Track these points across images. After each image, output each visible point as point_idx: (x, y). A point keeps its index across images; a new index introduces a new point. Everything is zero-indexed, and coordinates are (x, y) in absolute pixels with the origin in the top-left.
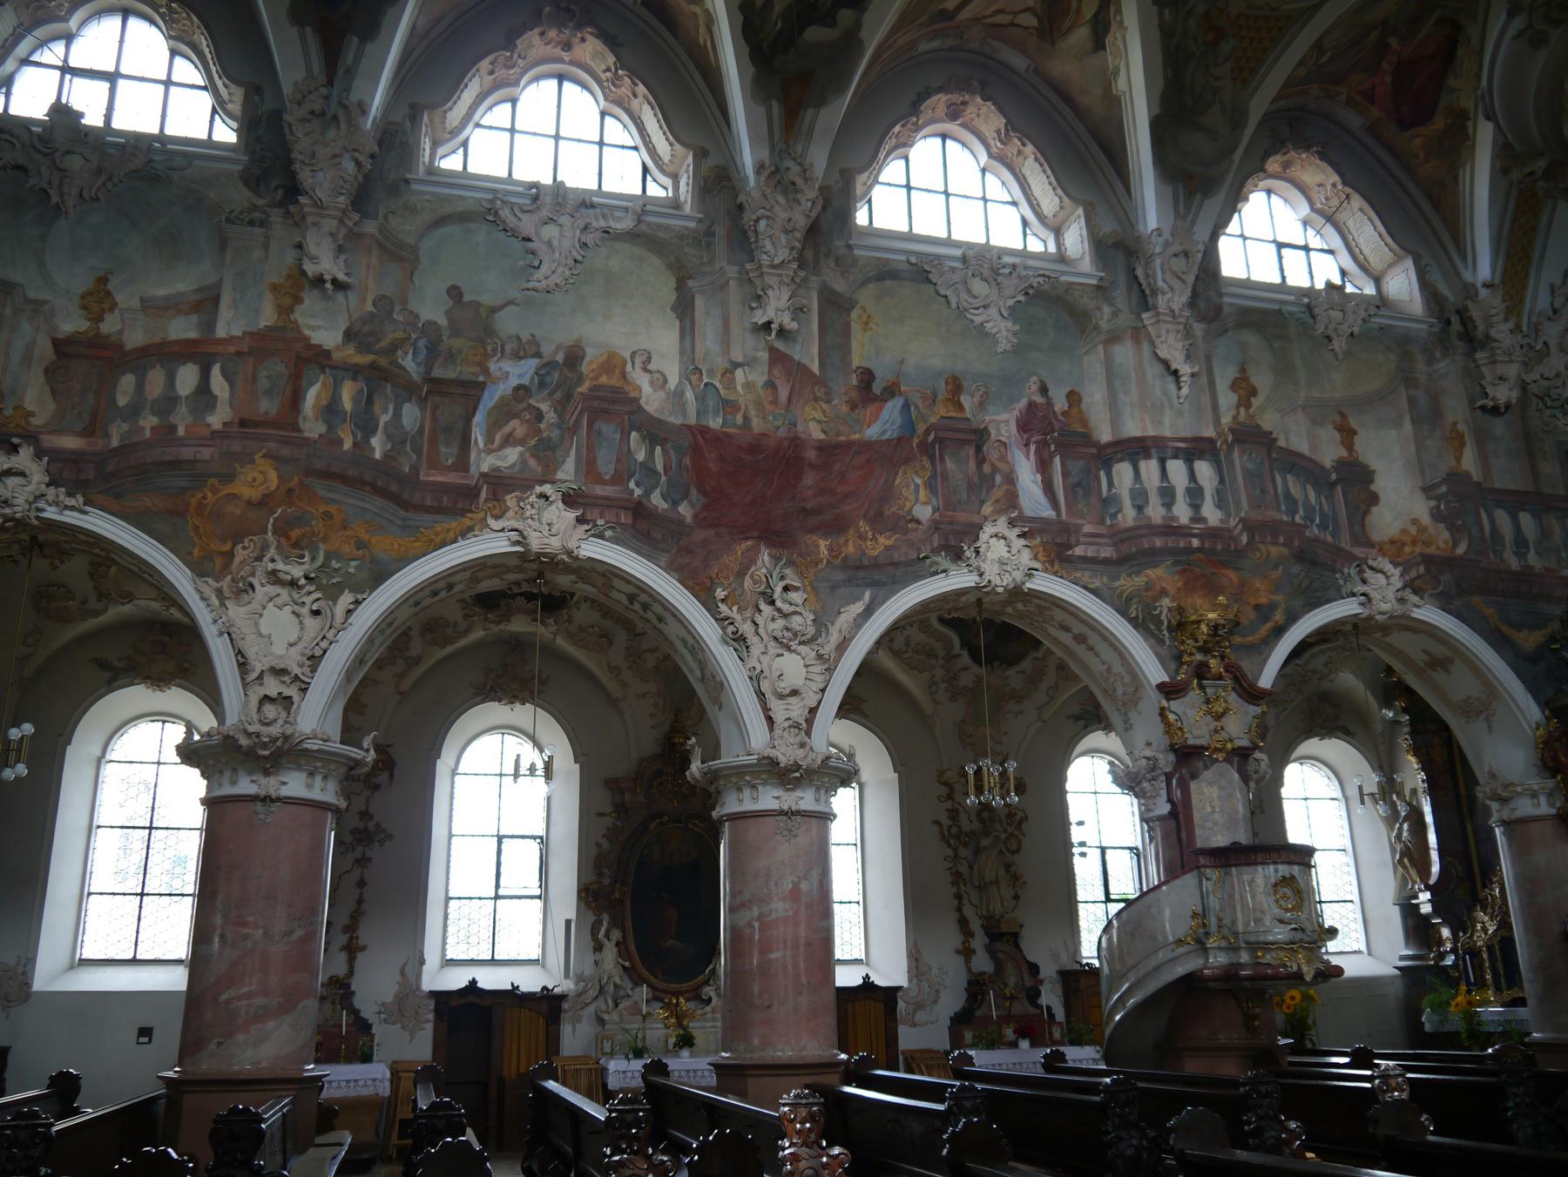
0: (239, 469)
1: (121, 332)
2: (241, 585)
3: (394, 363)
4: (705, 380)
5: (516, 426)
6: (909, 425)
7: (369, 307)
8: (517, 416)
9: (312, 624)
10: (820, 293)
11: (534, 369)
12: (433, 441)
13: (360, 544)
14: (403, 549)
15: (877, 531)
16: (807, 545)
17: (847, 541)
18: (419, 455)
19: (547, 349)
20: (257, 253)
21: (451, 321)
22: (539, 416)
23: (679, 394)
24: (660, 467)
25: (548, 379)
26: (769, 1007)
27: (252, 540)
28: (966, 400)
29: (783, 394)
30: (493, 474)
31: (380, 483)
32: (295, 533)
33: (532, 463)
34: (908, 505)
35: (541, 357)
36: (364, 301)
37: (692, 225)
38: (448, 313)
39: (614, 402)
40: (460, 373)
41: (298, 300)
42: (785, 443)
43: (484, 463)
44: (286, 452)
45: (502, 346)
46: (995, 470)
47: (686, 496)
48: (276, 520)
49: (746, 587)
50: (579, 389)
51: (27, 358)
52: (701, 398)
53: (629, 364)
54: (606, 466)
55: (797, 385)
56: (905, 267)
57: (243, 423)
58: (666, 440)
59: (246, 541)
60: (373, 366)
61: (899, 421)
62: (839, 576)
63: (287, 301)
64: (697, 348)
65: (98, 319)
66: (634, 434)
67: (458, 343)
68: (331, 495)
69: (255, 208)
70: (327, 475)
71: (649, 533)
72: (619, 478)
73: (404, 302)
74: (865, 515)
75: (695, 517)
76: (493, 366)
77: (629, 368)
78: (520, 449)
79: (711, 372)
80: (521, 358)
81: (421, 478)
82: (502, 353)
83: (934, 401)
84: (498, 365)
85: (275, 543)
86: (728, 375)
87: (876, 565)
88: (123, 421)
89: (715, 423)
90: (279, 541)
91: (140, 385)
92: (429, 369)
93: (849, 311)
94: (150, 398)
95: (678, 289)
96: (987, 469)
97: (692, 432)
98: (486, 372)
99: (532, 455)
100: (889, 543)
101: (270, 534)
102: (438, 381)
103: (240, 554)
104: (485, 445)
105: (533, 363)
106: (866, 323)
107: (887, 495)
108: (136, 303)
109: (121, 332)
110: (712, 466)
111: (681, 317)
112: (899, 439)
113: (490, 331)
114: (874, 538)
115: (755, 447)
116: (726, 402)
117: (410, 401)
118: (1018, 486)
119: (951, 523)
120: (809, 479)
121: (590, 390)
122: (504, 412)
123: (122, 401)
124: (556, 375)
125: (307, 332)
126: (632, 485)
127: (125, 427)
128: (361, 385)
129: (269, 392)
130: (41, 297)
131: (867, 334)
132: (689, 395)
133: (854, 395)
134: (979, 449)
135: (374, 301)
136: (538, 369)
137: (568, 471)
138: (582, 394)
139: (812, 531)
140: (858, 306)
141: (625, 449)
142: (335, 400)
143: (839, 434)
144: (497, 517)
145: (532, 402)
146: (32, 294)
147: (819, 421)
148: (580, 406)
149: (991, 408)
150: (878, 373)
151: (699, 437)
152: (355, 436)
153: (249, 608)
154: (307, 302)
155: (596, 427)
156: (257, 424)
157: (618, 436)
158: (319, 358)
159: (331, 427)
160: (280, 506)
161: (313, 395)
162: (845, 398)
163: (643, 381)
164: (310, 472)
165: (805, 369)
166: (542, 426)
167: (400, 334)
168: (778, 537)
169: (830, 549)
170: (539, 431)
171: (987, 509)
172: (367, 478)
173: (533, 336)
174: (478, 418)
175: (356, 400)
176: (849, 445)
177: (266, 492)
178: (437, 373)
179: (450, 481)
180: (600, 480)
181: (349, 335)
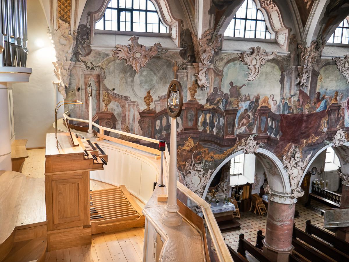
0: (185, 143)
1: (155, 108)
2: (187, 172)
3: (218, 107)
4: (285, 101)
5: (244, 121)
6: (326, 107)
7: (212, 91)
8: (244, 118)
9: (203, 179)
10: (312, 72)
11: (249, 104)
12: (227, 128)
13: (212, 157)
14: (221, 157)
15: (315, 136)
16: (302, 142)
17: (309, 139)
18: (224, 132)
19: (252, 98)
20: (185, 78)
21: (231, 93)
22: (249, 117)
23: (279, 106)
24: (274, 127)
25: (252, 107)
26: (283, 241)
27: (189, 160)
28: (338, 98)
29: (301, 103)
30: (240, 134)
31: (215, 141)
32: (198, 157)
33: (247, 130)
34: (323, 128)
35: (250, 100)
36: (211, 90)
37: (286, 55)
38: (230, 90)
39: (265, 110)
40: (233, 107)
41: (195, 92)
42: (300, 116)
43: (238, 132)
44: (195, 136)
45: (242, 98)
46: (341, 116)
47: (278, 133)
48: (194, 154)
49: (289, 154)
50: (258, 108)
51: (134, 119)
52: (284, 107)
53: (269, 99)
54: (263, 129)
55: (304, 100)
56: (331, 61)
57: (185, 130)
58: (275, 119)
59: (188, 161)
60: (213, 109)
61: (324, 106)
62: (307, 148)
63: (193, 92)
64: (284, 92)
65: (149, 105)
66: (269, 119)
67: (232, 99)
68: (205, 146)
69: (184, 64)
70: (204, 141)
71: (270, 144)
72: (265, 131)
73: (220, 88)
74: (314, 132)
75: (280, 138)
76: (240, 104)
77: (269, 100)
78: (245, 127)
79: (286, 99)
80: (246, 101)
81: (224, 138)
82: (242, 100)
83: (332, 99)
84: (241, 104)
85: (194, 160)
86: (290, 99)
87: (315, 144)
88: (158, 134)
89: (286, 113)
90: (195, 160)
91: (161, 123)
92: (226, 107)
93: (318, 76)
94: (164, 126)
95: (281, 75)
96: (339, 116)
97: (281, 117)
98: (238, 106)
99: (247, 128)
100: (318, 139)
101: (193, 158)
102: (228, 111)
103: (187, 164)
104: (238, 127)
105: (249, 102)
106: (321, 79)
107: (319, 126)
108: (157, 99)
109: (155, 108)
110: (285, 125)
111: (281, 84)
112: (323, 111)
113: (239, 94)
114: (315, 138)
115: (294, 118)
116: (289, 107)
117: (221, 117)
118: (345, 120)
119: (330, 131)
120: (304, 125)
121: (261, 108)
122: (242, 117)
123: (157, 128)
124: (253, 105)
125: (198, 101)
126: (268, 132)
127: (159, 135)
128: (211, 114)
129: (190, 120)
130: (134, 100)
131: (321, 83)
132: (281, 106)
133: (316, 100)
134: (339, 111)
135: (213, 89)
136: (250, 104)
137: (254, 131)
138: (259, 109)
139: (303, 138)
140: (320, 74)
141: (267, 123)
142: (205, 119)
143: (311, 112)
144: (240, 146)
145: (248, 113)
146: (132, 100)
147: (307, 109)
148: (258, 113)
149: (343, 99)
150: (321, 94)
151: (283, 117)
152: (210, 129)
153: (190, 177)
154: (198, 92)
155: (261, 118)
156: (188, 129)
157: (265, 120)
158: (200, 109)
159: (205, 128)
160: (194, 151)
161: (201, 119)
162: (314, 102)
163: (271, 103)
164: (200, 141)
165: (306, 94)
166: (250, 120)
167: (219, 98)
168: (296, 141)
169: (306, 142)
170: (249, 121)
171: (338, 127)
172: (213, 140)
173: (249, 94)
174: (236, 120)
175: (210, 119)
176: (313, 114)
177: (191, 147)
178: (228, 108)
179: (231, 138)
180: (261, 132)
181: (208, 100)
